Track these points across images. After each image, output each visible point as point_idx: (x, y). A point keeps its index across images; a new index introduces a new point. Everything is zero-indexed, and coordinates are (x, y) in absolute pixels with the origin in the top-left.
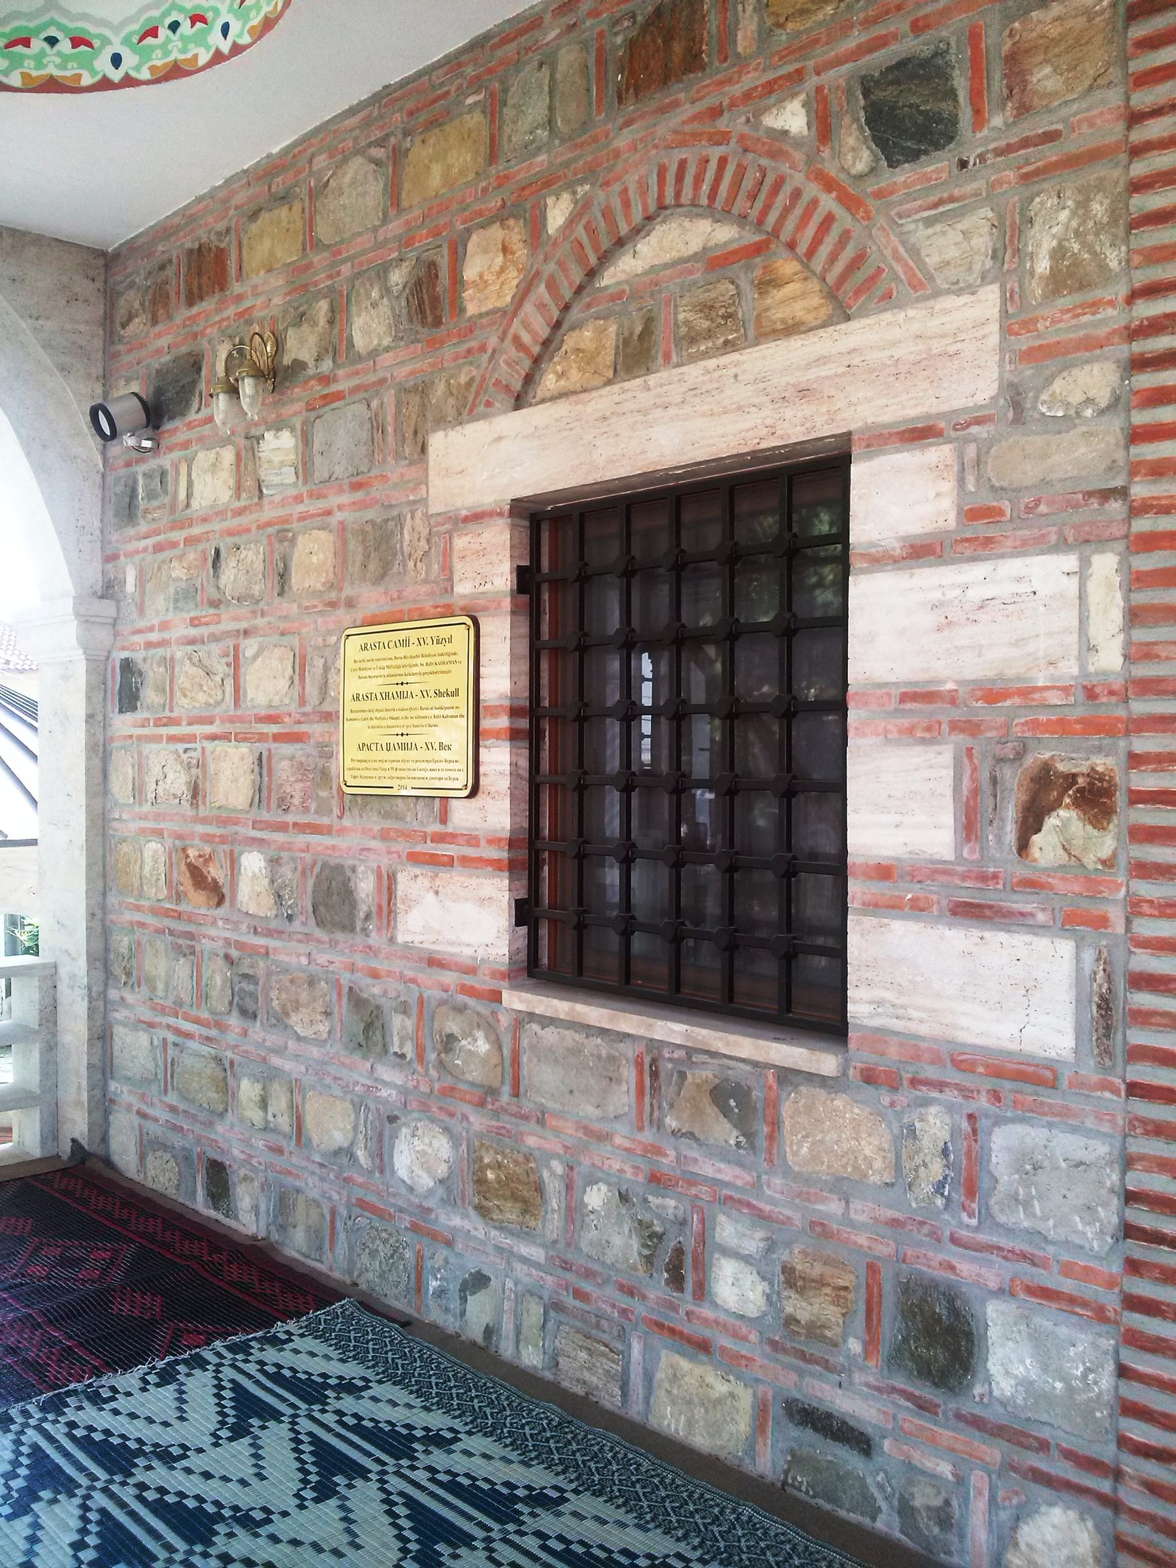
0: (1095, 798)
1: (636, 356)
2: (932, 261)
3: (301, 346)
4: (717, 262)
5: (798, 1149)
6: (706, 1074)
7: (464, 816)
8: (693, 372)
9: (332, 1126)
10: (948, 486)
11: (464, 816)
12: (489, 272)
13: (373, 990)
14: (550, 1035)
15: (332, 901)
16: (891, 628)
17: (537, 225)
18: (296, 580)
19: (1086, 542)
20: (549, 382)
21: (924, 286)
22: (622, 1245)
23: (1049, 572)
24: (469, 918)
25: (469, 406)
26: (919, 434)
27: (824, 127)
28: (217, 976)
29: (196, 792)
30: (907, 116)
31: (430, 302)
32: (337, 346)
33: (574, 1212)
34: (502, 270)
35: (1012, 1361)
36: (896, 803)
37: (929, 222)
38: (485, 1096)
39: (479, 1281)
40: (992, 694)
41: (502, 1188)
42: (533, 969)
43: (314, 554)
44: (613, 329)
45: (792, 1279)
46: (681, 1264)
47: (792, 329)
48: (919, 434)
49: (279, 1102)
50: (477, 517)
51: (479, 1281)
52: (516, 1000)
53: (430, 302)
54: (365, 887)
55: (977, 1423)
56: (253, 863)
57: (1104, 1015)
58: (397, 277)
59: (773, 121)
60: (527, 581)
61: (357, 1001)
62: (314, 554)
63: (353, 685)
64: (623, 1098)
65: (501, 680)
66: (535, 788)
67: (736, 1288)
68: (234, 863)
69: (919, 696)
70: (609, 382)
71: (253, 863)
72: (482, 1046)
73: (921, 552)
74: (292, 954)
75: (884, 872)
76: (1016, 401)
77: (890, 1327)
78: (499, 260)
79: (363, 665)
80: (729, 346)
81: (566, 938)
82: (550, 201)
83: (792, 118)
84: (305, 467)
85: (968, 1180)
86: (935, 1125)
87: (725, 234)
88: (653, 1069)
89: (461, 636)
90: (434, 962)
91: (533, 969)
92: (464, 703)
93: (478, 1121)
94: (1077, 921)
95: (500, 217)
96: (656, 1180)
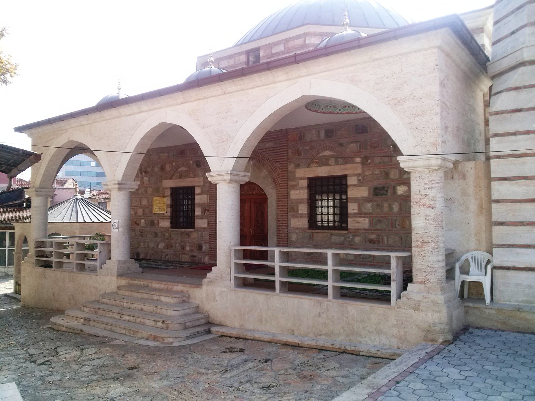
0: (208, 210)
1: (180, 177)
3: (149, 170)
4: (186, 171)
5: (192, 237)
6: (186, 232)
7: (166, 214)
9: (152, 245)
11: (166, 214)
12: (168, 167)
13: (157, 231)
14: (173, 232)
15: (152, 223)
16: (198, 199)
18: (148, 192)
19: (207, 195)
20: (173, 178)
22: (179, 248)
23: (205, 196)
24: (166, 224)
25: (166, 178)
27: (193, 163)
28: (138, 233)
29: (135, 214)
31: (162, 168)
32: (153, 170)
33: (175, 246)
35: (204, 248)
36: (198, 212)
38: (168, 239)
39: (167, 255)
40: (203, 204)
41: (169, 246)
42: (172, 227)
43: (150, 190)
45: (191, 246)
46: (183, 248)
48: (199, 186)
49: (146, 244)
50: (167, 188)
51: (167, 255)
52: (171, 230)
53: (162, 168)
54: (156, 222)
55: (202, 253)
56: (143, 221)
57: (208, 224)
58: (159, 165)
60: (171, 194)
61: (155, 233)
62: (150, 190)
63: (154, 203)
64: (179, 236)
65: (169, 203)
66: (172, 212)
67: (188, 248)
68: (140, 221)
69: (199, 204)
71: (143, 221)
72: (167, 234)
73: (199, 194)
74: (148, 229)
75: (197, 216)
76: (204, 185)
77: (198, 248)
79: (156, 200)
81: (175, 224)
83: (191, 162)
84: (149, 181)
85: (202, 236)
86: (200, 233)
88: (182, 233)
89: (165, 199)
90: (163, 228)
91: (172, 227)
92: (166, 204)
93: (167, 241)
94: (207, 218)
95: (169, 163)
96: (182, 242)
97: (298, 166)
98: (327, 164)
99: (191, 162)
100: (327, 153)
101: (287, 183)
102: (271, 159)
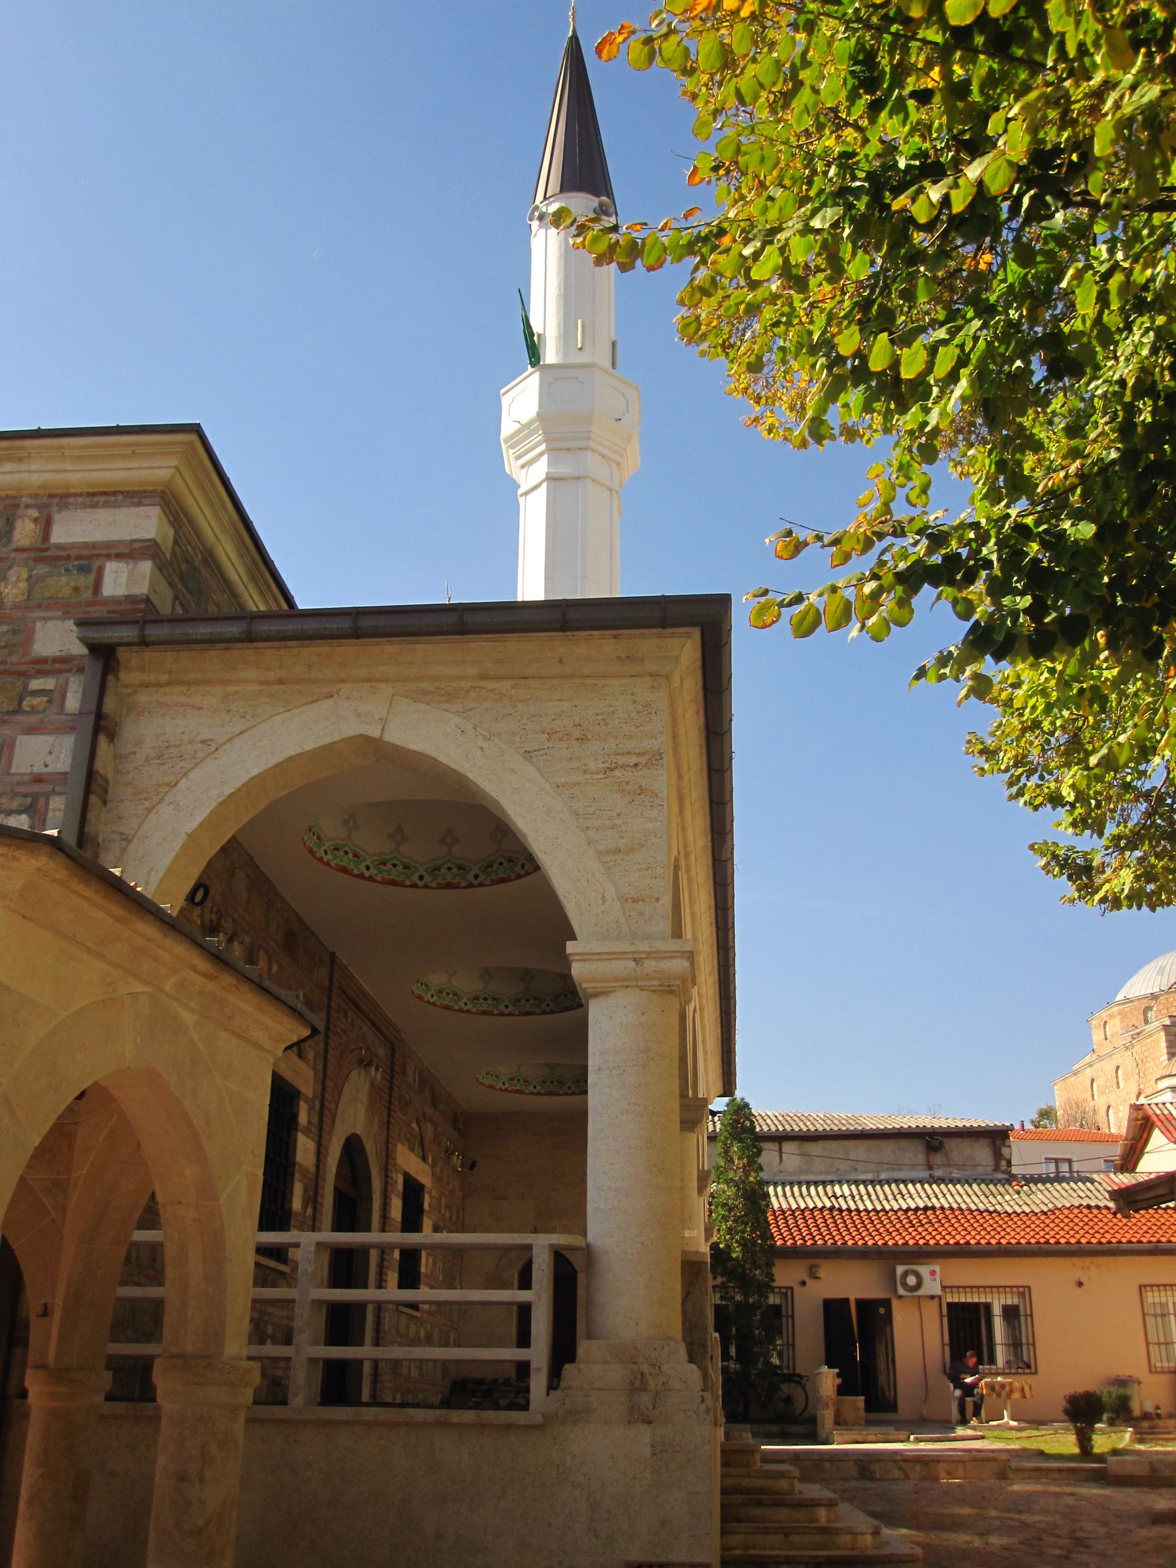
98: (413, 1150)
100: (414, 1125)
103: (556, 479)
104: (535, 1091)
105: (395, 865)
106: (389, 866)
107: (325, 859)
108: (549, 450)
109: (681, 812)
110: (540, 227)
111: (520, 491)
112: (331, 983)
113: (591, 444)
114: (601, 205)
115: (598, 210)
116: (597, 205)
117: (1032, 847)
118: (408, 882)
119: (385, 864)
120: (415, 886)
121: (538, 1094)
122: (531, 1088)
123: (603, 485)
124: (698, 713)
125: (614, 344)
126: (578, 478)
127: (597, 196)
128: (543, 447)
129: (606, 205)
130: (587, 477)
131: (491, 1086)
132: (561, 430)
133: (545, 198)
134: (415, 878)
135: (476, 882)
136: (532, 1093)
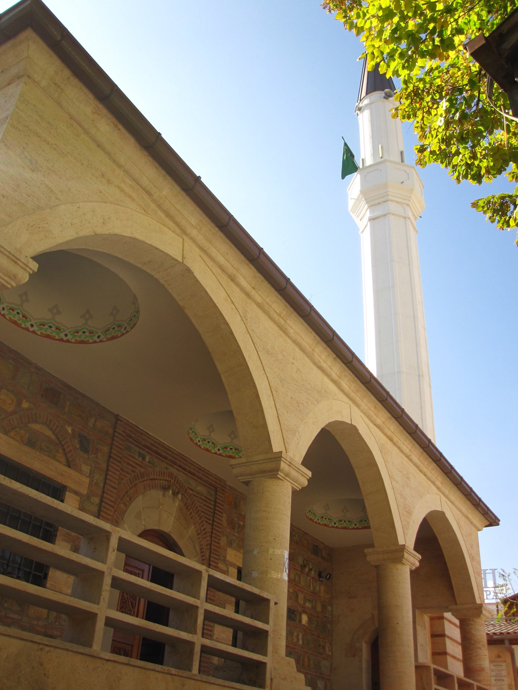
2: (83, 469)
8: (45, 458)
10: (78, 503)
17: (19, 403)
21: (80, 471)
26: (76, 493)
30: (85, 445)
34: (10, 404)
37: (83, 463)
44: (28, 435)
47: (60, 462)
59: (66, 426)
70: (24, 444)
78: (10, 402)
80: (49, 456)
82: (24, 401)
83: (70, 430)
87: (53, 437)
97: (230, 544)
99: (70, 430)
101: (217, 563)
102: (202, 514)
103: (374, 219)
104: (356, 527)
105: (84, 332)
106: (81, 333)
107: (31, 329)
108: (370, 207)
109: (184, 232)
110: (360, 113)
111: (360, 231)
112: (115, 431)
113: (390, 197)
114: (386, 94)
115: (386, 96)
116: (384, 95)
117: (475, 205)
118: (91, 341)
119: (78, 332)
120: (95, 342)
121: (358, 528)
122: (353, 526)
123: (400, 216)
124: (116, 126)
125: (402, 153)
126: (385, 215)
127: (383, 90)
128: (366, 206)
129: (389, 93)
130: (389, 213)
131: (325, 525)
132: (375, 197)
133: (360, 100)
134: (95, 338)
135: (124, 332)
136: (354, 528)
